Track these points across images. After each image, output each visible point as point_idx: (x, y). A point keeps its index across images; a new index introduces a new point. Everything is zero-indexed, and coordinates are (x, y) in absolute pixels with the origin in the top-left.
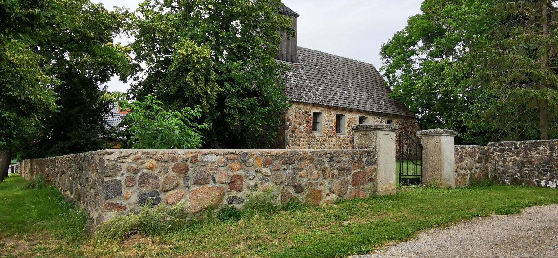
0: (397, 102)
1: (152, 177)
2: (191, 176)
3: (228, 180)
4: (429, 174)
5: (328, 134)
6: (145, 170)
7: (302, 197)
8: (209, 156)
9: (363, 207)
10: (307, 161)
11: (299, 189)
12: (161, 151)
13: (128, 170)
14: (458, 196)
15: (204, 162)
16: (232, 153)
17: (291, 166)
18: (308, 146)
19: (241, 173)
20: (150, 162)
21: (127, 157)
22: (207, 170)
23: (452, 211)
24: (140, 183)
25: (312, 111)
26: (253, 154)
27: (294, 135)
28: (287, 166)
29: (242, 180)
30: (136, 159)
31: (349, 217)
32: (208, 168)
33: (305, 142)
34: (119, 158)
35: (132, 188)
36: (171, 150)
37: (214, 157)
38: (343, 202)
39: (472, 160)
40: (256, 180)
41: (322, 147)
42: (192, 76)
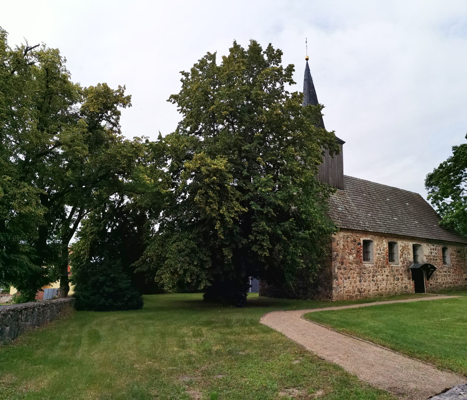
0: (449, 228)
18: (358, 278)
25: (362, 239)
27: (342, 267)
33: (355, 275)
41: (375, 279)
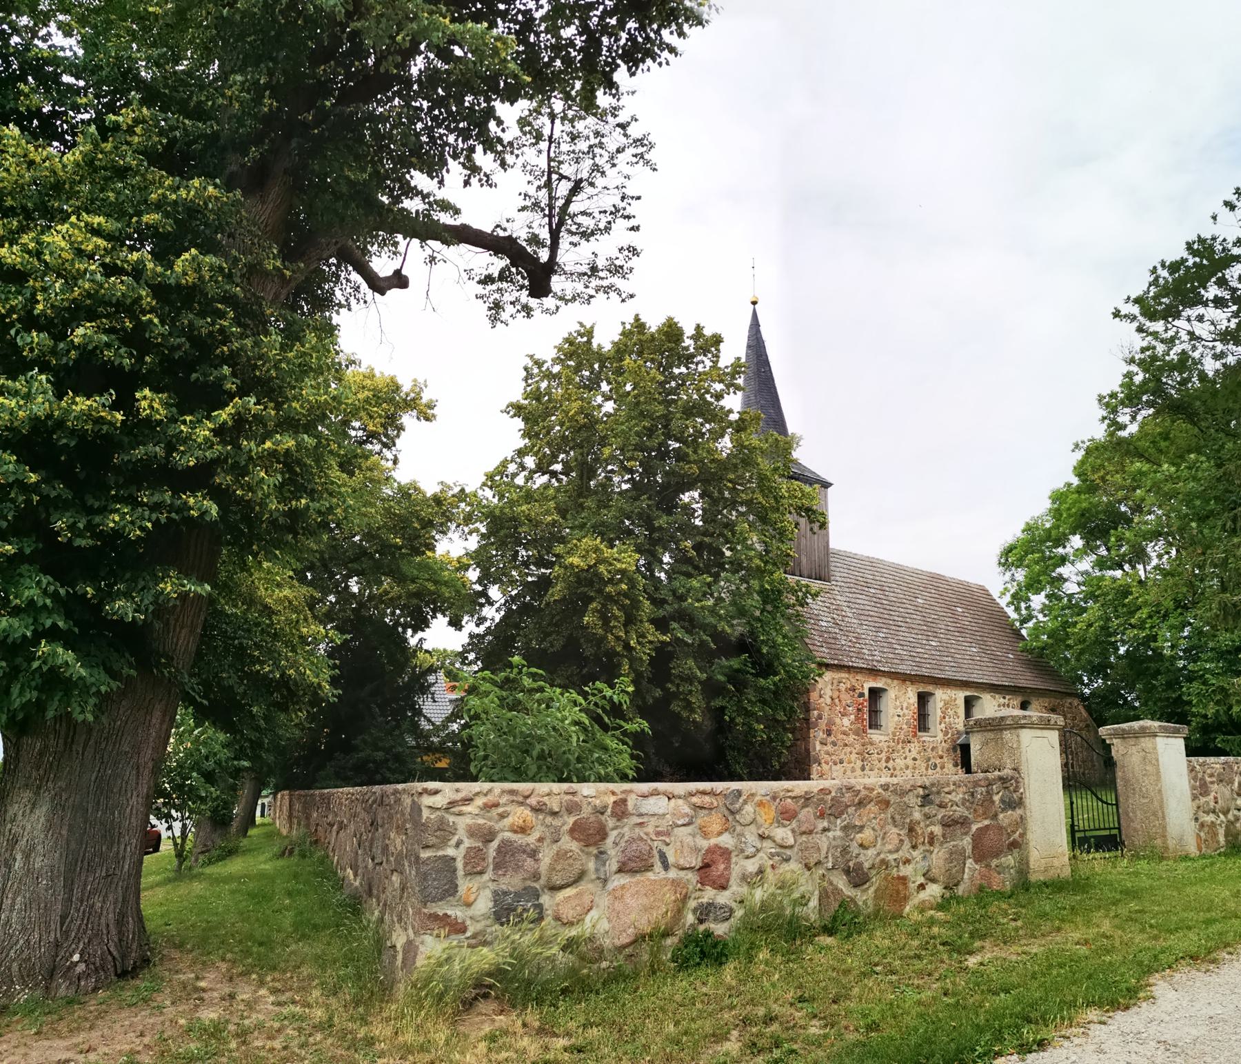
1: (524, 852)
2: (612, 852)
3: (696, 862)
4: (1136, 825)
5: (902, 737)
6: (508, 835)
7: (864, 898)
8: (652, 800)
9: (1004, 915)
10: (873, 807)
11: (858, 877)
12: (544, 787)
13: (472, 832)
14: (1212, 878)
15: (641, 815)
16: (704, 793)
17: (839, 821)
19: (726, 840)
20: (520, 814)
21: (468, 800)
22: (647, 834)
23: (1215, 920)
24: (497, 867)
26: (752, 795)
28: (829, 822)
29: (728, 860)
30: (488, 807)
31: (977, 944)
32: (650, 829)
34: (453, 803)
35: (478, 878)
36: (565, 786)
37: (663, 803)
38: (958, 903)
39: (1226, 791)
40: (761, 858)
42: (598, 611)
